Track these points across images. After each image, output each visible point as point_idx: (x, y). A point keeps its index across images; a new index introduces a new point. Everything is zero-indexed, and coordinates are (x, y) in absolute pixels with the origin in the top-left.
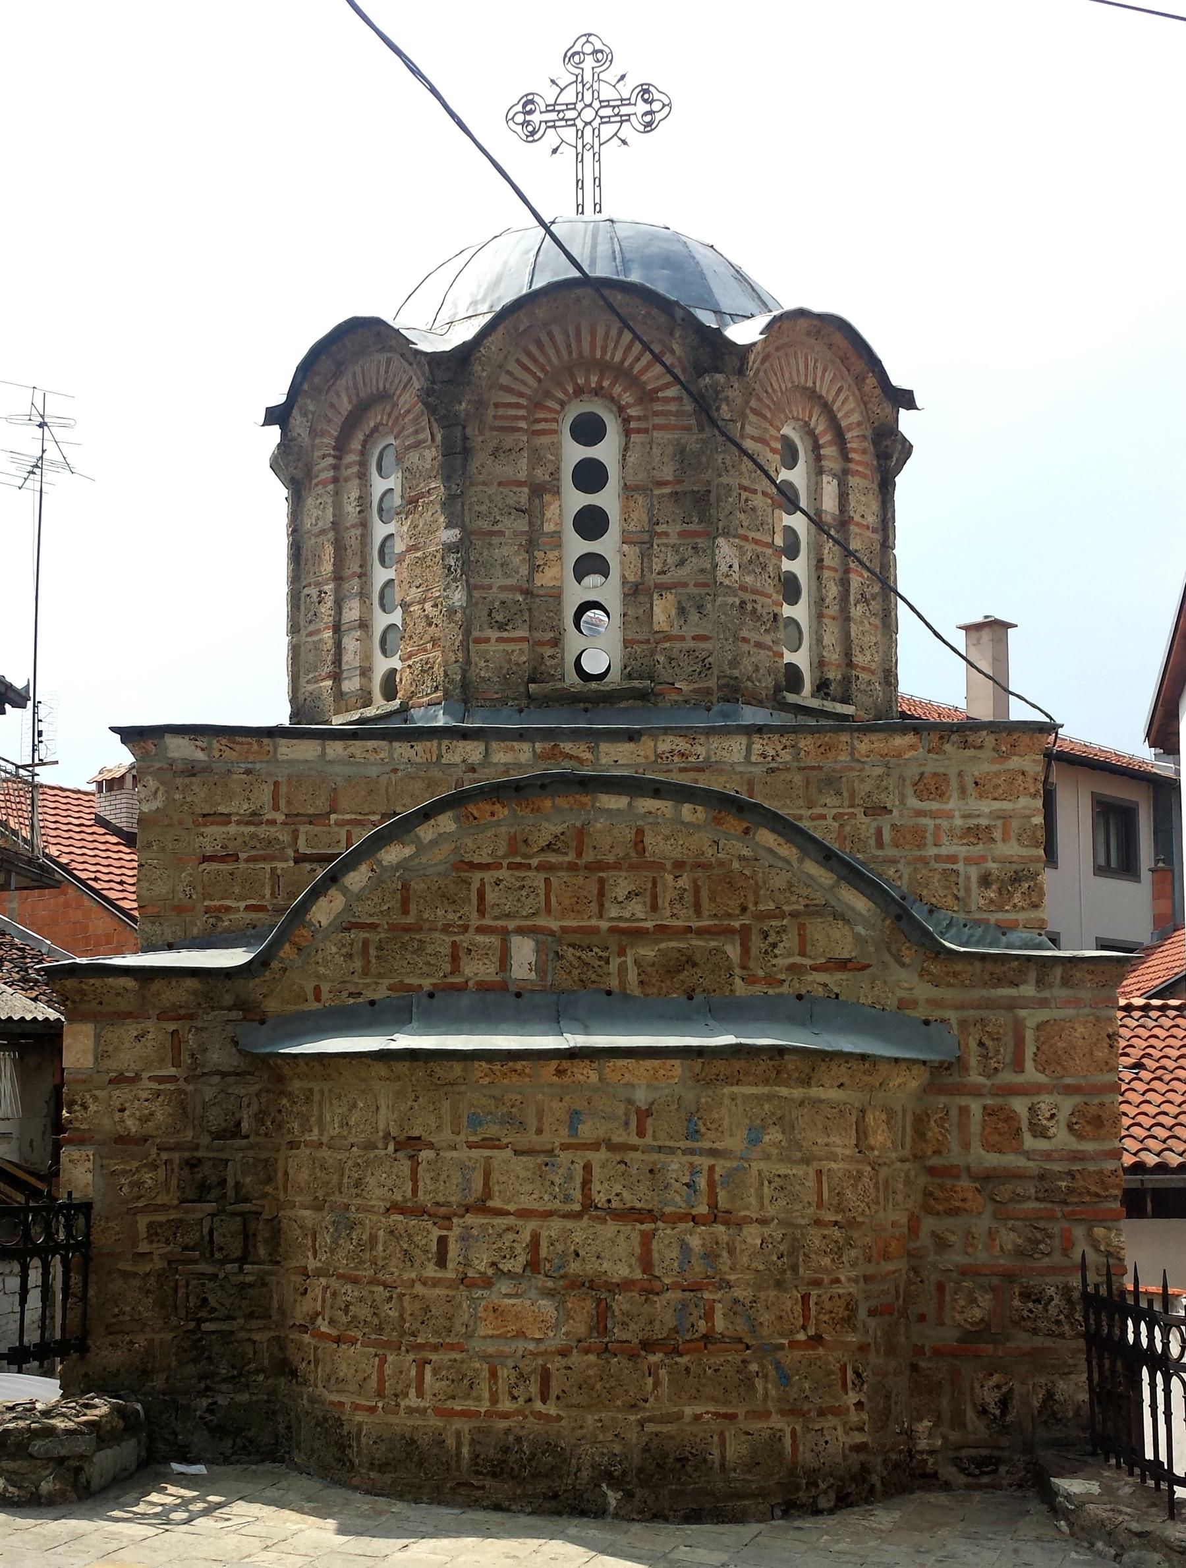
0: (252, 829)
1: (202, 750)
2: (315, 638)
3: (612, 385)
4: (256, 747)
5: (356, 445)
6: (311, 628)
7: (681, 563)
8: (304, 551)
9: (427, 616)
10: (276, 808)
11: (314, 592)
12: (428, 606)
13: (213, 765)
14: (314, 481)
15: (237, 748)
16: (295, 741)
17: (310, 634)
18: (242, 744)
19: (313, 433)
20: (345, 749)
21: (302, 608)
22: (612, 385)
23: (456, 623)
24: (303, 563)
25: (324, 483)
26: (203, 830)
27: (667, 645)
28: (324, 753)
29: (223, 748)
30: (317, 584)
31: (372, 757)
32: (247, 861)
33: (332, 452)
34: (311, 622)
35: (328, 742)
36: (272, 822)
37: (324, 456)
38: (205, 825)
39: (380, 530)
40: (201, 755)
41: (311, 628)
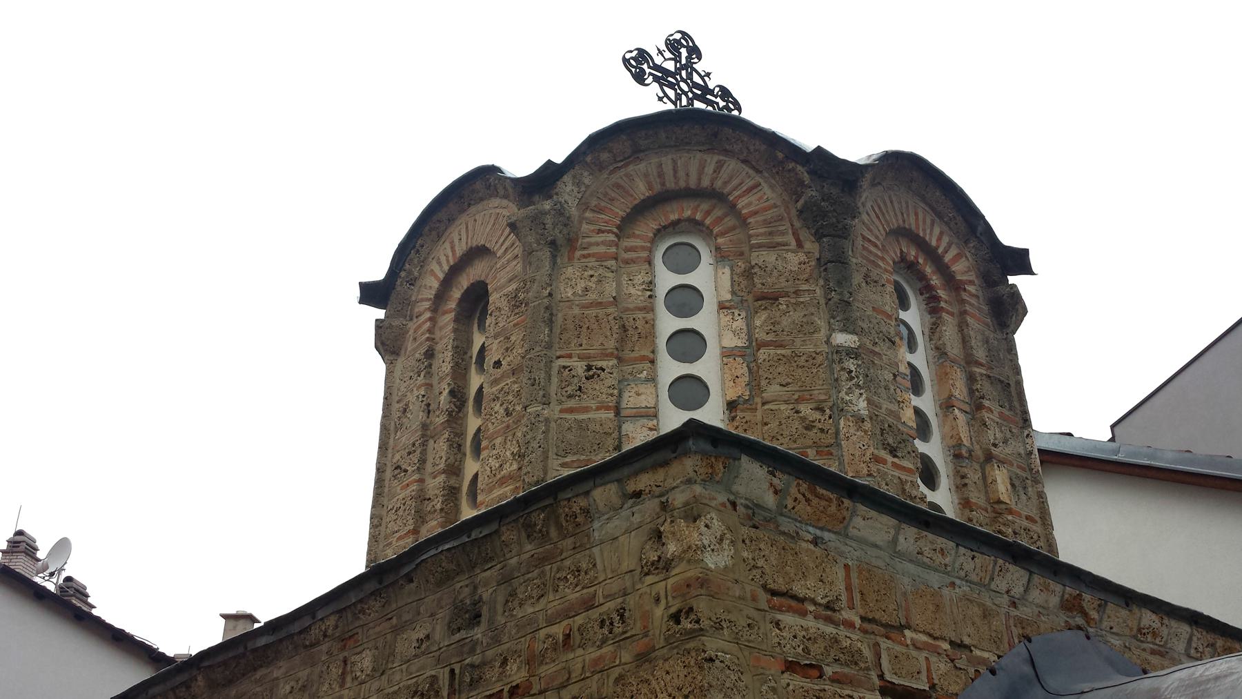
0: (829, 629)
1: (776, 492)
2: (584, 416)
3: (957, 257)
4: (833, 508)
5: (647, 227)
6: (572, 403)
7: (1005, 442)
8: (559, 318)
9: (803, 419)
10: (852, 607)
11: (579, 367)
12: (806, 409)
13: (781, 519)
14: (578, 253)
15: (815, 501)
16: (873, 513)
17: (571, 410)
18: (820, 497)
19: (584, 205)
20: (917, 540)
21: (555, 380)
22: (957, 257)
23: (865, 432)
24: (557, 330)
25: (601, 258)
26: (779, 616)
27: (1010, 518)
28: (895, 541)
29: (800, 497)
30: (581, 358)
31: (939, 559)
32: (836, 680)
33: (615, 230)
34: (570, 396)
35: (904, 526)
36: (850, 625)
37: (600, 231)
38: (780, 610)
39: (668, 324)
40: (770, 500)
41: (572, 403)
